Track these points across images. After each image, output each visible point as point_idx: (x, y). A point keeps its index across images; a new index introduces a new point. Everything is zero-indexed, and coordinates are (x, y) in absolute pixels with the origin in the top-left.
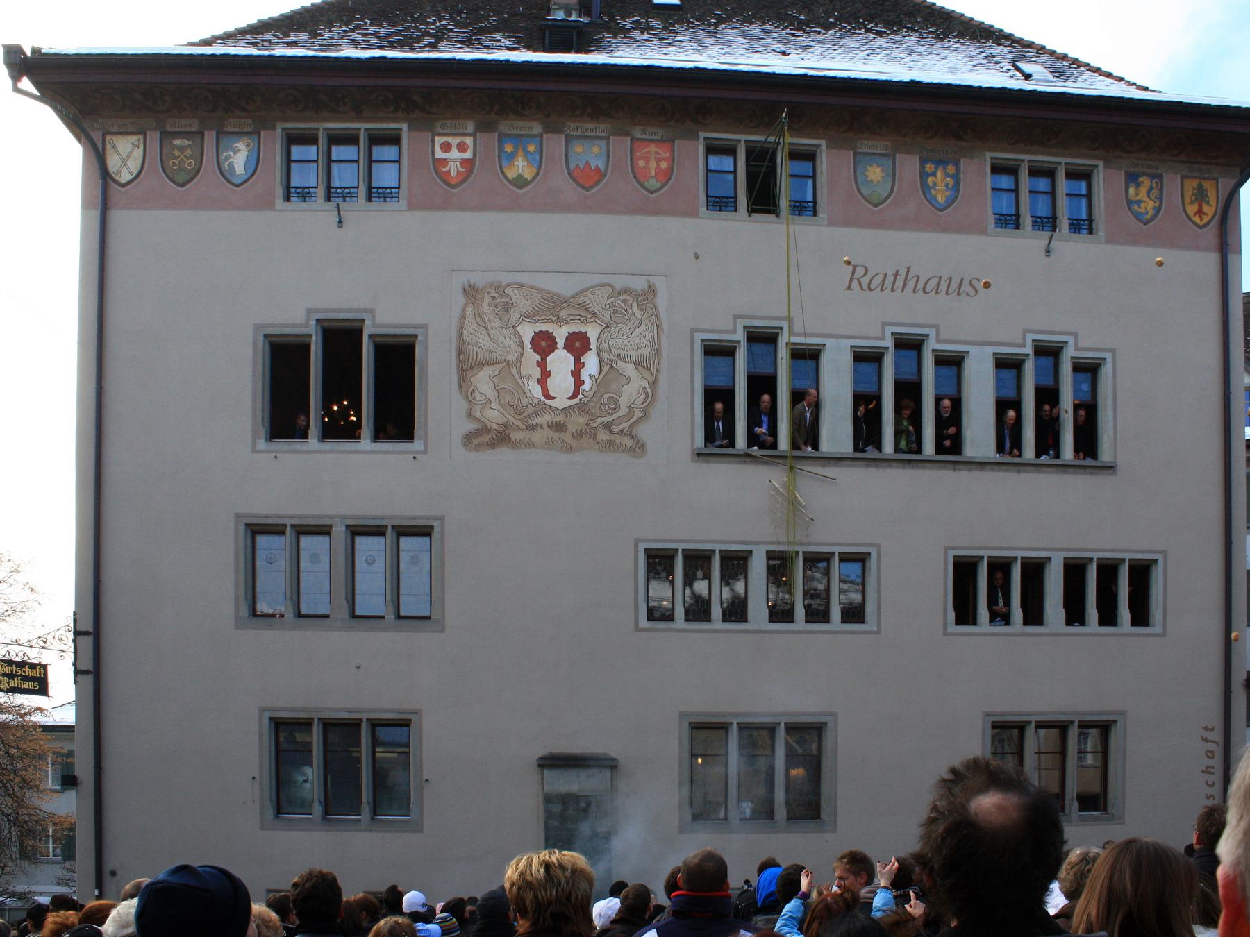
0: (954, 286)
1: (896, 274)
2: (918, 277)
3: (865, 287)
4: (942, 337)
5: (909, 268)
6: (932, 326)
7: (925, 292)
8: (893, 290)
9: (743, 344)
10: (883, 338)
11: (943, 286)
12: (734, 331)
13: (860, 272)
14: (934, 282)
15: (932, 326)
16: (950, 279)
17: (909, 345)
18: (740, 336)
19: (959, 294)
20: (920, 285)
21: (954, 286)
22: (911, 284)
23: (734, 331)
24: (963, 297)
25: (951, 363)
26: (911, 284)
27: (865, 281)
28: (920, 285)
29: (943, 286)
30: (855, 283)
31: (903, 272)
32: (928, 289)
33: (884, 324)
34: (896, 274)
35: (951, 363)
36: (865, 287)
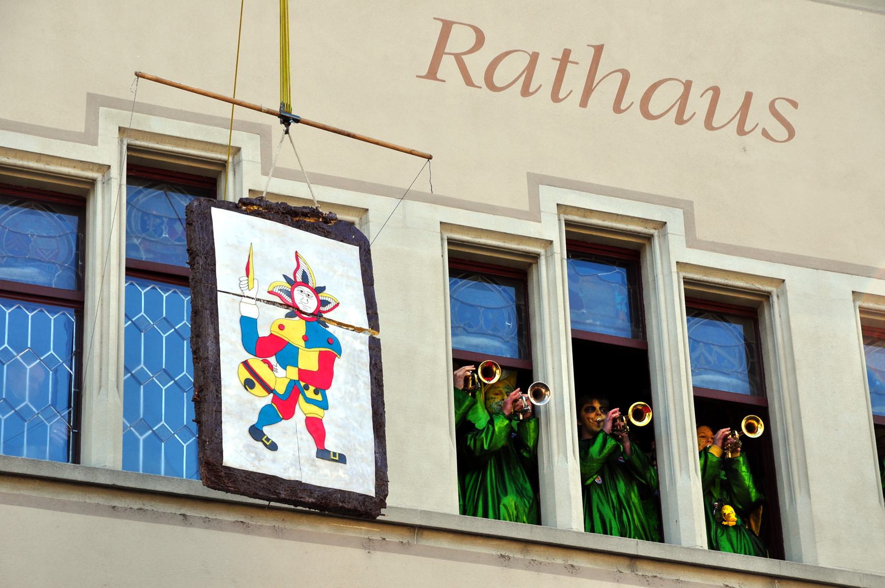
0: (727, 109)
1: (565, 59)
3: (478, 77)
4: (702, 233)
5: (599, 50)
6: (672, 203)
7: (647, 115)
8: (555, 98)
9: (118, 175)
10: (534, 215)
11: (698, 105)
12: (90, 137)
13: (461, 39)
15: (672, 203)
16: (716, 91)
17: (611, 253)
18: (110, 153)
19: (741, 131)
20: (634, 94)
21: (727, 109)
23: (90, 137)
24: (754, 139)
25: (732, 311)
27: (477, 64)
28: (634, 94)
29: (698, 105)
30: (448, 65)
31: (583, 57)
32: (654, 108)
34: (565, 59)
35: (732, 311)
36: (478, 77)
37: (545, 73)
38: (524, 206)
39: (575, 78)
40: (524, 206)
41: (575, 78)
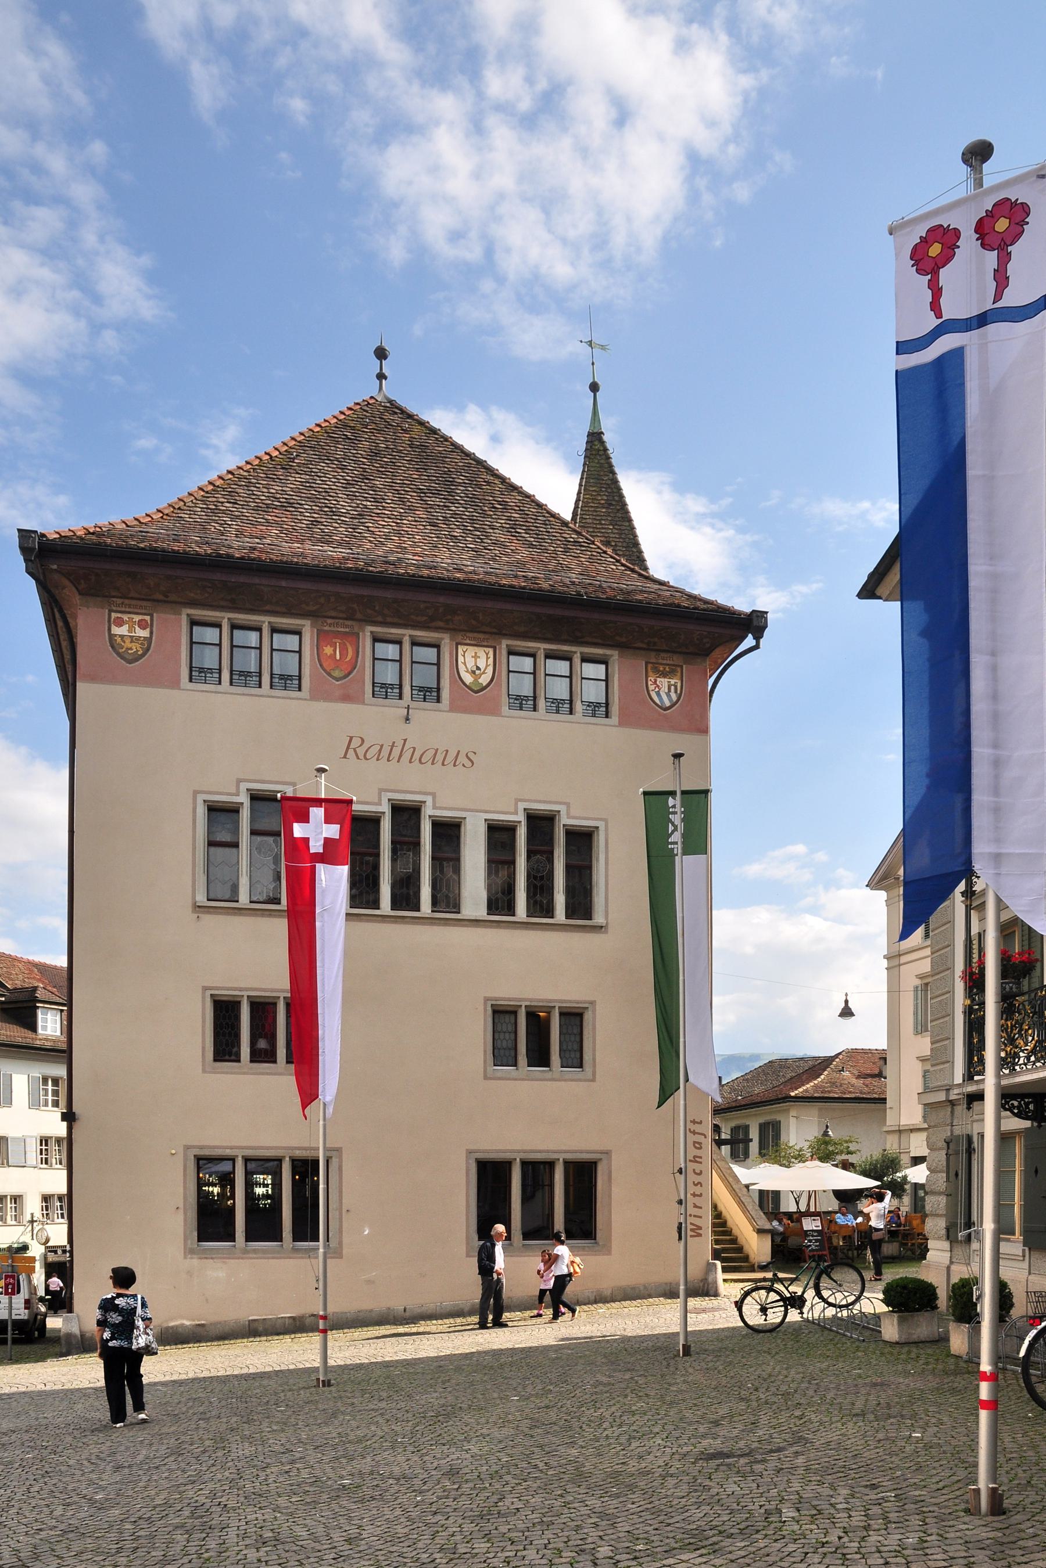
0: (450, 758)
1: (393, 746)
2: (414, 749)
5: (405, 740)
8: (388, 760)
11: (440, 757)
14: (431, 753)
16: (447, 751)
19: (455, 765)
21: (450, 758)
22: (407, 755)
26: (407, 755)
29: (440, 757)
32: (423, 761)
33: (381, 791)
34: (393, 746)
37: (385, 753)
38: (376, 801)
39: (396, 752)
40: (376, 801)
41: (396, 752)
